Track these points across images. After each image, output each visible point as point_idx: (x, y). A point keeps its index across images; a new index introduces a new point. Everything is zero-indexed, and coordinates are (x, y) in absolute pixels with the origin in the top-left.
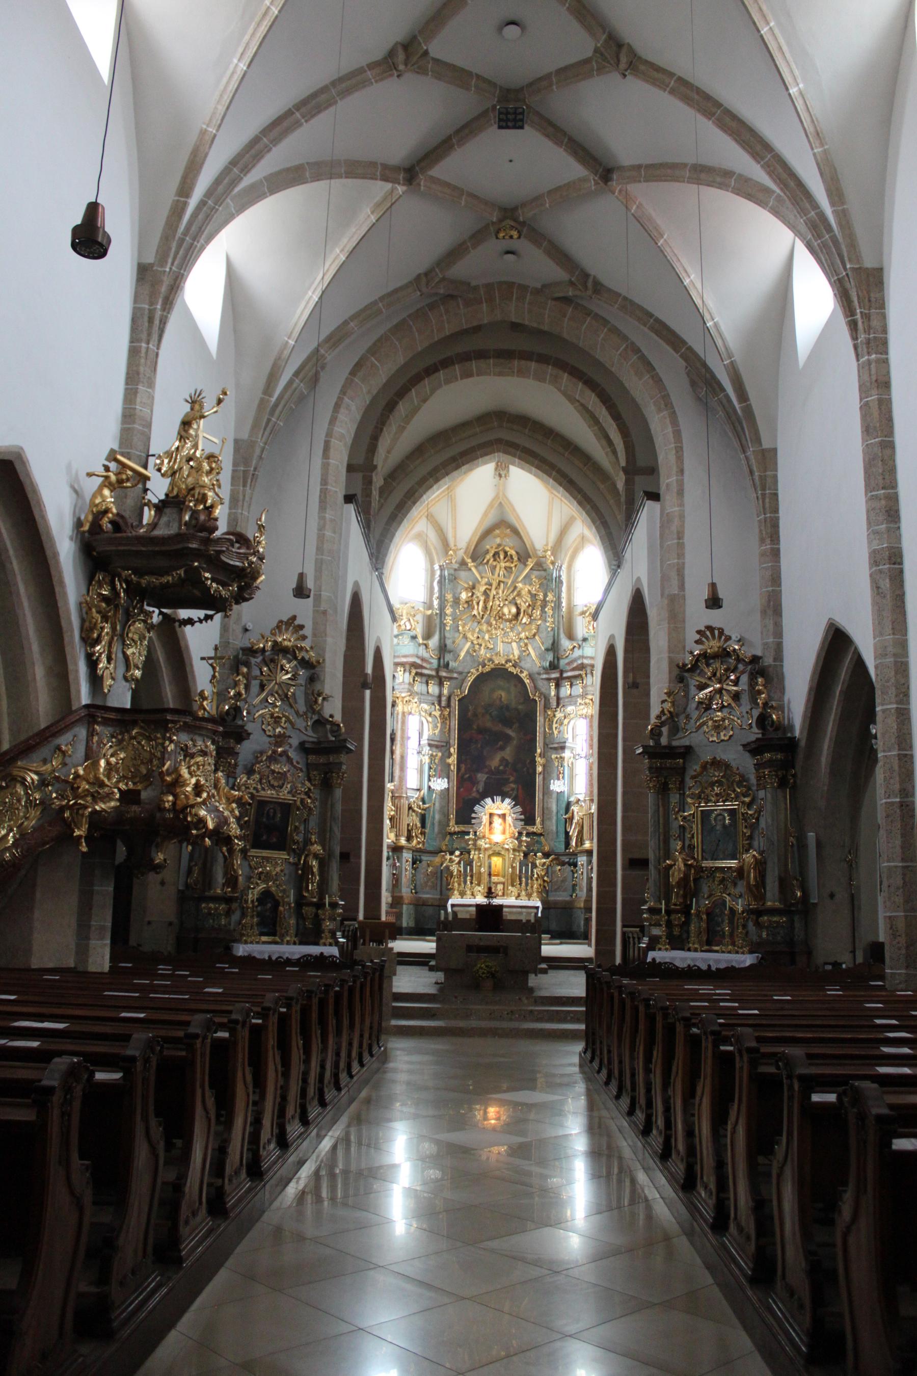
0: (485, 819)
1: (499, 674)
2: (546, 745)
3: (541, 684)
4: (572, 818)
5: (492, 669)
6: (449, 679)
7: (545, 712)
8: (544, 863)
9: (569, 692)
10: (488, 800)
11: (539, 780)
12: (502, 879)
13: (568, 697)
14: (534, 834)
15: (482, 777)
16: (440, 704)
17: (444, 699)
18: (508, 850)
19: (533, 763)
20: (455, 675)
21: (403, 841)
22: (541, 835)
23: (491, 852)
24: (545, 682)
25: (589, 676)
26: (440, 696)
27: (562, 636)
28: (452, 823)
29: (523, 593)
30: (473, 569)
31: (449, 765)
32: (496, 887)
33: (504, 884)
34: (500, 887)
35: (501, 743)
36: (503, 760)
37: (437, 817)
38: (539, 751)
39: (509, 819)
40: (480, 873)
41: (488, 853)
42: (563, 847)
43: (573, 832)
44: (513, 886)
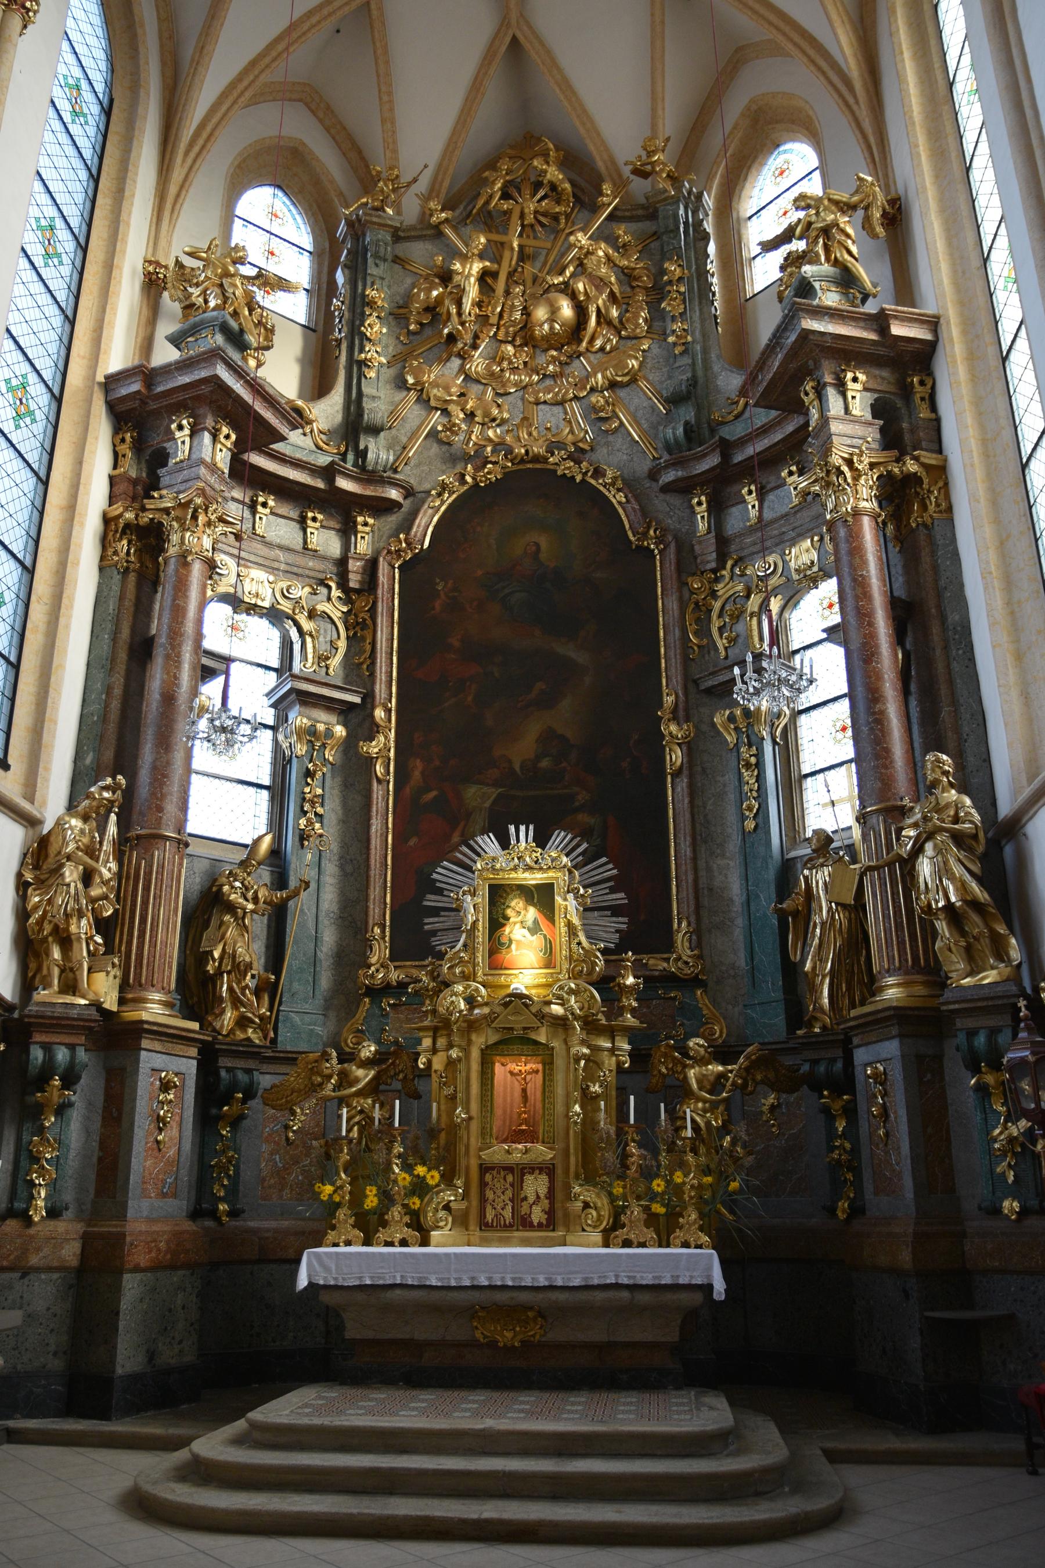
0: (474, 909)
1: (529, 485)
2: (690, 682)
3: (661, 504)
4: (804, 915)
5: (508, 475)
6: (381, 507)
7: (683, 584)
8: (722, 1076)
9: (753, 513)
10: (490, 844)
11: (675, 793)
12: (541, 1152)
13: (752, 530)
14: (670, 980)
15: (478, 796)
16: (343, 585)
17: (354, 565)
18: (561, 1024)
19: (655, 744)
20: (394, 494)
21: (154, 1009)
22: (696, 982)
23: (493, 1038)
24: (675, 500)
25: (831, 393)
26: (342, 563)
27: (716, 368)
28: (379, 952)
29: (590, 263)
30: (448, 231)
31: (369, 761)
32: (518, 1185)
33: (548, 1170)
34: (535, 1186)
35: (540, 686)
36: (548, 737)
37: (329, 937)
38: (669, 700)
39: (568, 905)
40: (453, 1128)
41: (479, 1041)
42: (779, 1021)
43: (818, 961)
44: (589, 1178)
